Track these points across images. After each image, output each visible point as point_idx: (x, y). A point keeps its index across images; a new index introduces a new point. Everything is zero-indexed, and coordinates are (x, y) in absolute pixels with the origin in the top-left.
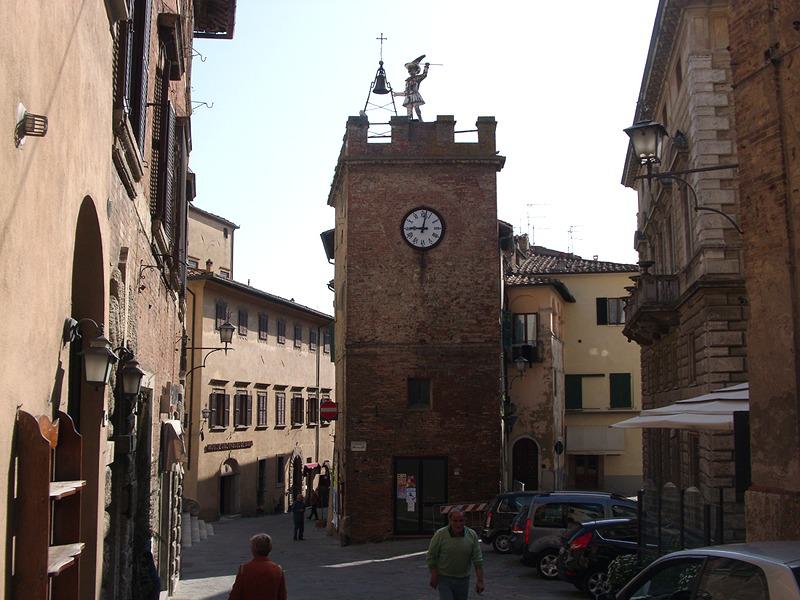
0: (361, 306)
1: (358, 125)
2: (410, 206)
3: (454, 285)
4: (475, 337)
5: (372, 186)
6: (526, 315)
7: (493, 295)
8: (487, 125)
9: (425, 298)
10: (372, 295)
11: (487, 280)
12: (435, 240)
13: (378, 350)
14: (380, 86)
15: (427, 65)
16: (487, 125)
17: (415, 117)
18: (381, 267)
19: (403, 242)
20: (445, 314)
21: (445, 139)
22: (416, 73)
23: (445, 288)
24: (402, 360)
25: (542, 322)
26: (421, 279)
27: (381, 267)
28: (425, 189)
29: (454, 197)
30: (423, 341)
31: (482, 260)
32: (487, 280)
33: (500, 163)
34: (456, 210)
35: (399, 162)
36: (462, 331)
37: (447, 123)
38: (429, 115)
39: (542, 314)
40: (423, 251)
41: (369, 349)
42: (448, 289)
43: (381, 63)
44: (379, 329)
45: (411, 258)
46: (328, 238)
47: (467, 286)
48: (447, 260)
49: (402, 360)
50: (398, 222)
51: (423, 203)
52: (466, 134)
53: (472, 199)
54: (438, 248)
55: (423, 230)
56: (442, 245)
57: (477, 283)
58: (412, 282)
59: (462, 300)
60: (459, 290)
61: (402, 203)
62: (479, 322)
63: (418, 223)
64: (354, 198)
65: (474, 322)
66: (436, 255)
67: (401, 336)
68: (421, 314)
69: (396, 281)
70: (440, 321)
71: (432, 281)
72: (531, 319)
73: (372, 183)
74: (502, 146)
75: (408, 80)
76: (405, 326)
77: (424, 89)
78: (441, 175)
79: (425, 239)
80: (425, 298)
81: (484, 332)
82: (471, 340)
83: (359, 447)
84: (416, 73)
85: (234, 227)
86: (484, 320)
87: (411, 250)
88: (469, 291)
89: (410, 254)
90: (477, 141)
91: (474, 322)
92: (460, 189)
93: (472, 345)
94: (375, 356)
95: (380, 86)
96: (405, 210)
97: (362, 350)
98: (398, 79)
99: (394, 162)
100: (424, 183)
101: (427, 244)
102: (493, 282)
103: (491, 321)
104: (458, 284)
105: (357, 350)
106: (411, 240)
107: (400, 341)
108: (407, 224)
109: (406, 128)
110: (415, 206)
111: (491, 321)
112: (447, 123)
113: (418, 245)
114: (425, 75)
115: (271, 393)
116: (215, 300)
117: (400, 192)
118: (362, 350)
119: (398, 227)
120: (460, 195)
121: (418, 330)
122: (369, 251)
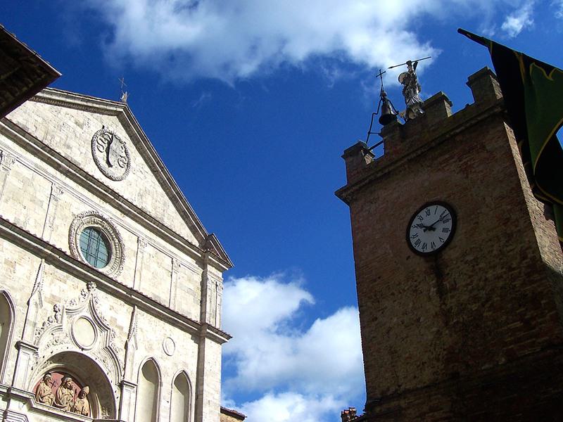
3: (482, 283)
7: (536, 277)
9: (446, 315)
10: (388, 332)
11: (524, 258)
12: (446, 236)
13: (403, 403)
18: (393, 294)
19: (412, 254)
21: (437, 120)
23: (473, 289)
24: (432, 410)
26: (441, 292)
27: (393, 294)
28: (427, 184)
37: (437, 102)
40: (437, 254)
42: (475, 292)
45: (424, 270)
47: (499, 278)
51: (427, 200)
54: (452, 244)
55: (432, 229)
57: (511, 269)
58: (430, 299)
59: (496, 299)
63: (428, 221)
65: (518, 324)
66: (451, 254)
67: (427, 376)
69: (411, 305)
71: (454, 288)
79: (434, 240)
87: (422, 260)
88: (501, 284)
89: (420, 265)
90: (471, 101)
91: (518, 324)
96: (409, 216)
99: (387, 171)
101: (439, 245)
102: (533, 259)
106: (419, 249)
110: (418, 207)
113: (429, 250)
119: (404, 240)
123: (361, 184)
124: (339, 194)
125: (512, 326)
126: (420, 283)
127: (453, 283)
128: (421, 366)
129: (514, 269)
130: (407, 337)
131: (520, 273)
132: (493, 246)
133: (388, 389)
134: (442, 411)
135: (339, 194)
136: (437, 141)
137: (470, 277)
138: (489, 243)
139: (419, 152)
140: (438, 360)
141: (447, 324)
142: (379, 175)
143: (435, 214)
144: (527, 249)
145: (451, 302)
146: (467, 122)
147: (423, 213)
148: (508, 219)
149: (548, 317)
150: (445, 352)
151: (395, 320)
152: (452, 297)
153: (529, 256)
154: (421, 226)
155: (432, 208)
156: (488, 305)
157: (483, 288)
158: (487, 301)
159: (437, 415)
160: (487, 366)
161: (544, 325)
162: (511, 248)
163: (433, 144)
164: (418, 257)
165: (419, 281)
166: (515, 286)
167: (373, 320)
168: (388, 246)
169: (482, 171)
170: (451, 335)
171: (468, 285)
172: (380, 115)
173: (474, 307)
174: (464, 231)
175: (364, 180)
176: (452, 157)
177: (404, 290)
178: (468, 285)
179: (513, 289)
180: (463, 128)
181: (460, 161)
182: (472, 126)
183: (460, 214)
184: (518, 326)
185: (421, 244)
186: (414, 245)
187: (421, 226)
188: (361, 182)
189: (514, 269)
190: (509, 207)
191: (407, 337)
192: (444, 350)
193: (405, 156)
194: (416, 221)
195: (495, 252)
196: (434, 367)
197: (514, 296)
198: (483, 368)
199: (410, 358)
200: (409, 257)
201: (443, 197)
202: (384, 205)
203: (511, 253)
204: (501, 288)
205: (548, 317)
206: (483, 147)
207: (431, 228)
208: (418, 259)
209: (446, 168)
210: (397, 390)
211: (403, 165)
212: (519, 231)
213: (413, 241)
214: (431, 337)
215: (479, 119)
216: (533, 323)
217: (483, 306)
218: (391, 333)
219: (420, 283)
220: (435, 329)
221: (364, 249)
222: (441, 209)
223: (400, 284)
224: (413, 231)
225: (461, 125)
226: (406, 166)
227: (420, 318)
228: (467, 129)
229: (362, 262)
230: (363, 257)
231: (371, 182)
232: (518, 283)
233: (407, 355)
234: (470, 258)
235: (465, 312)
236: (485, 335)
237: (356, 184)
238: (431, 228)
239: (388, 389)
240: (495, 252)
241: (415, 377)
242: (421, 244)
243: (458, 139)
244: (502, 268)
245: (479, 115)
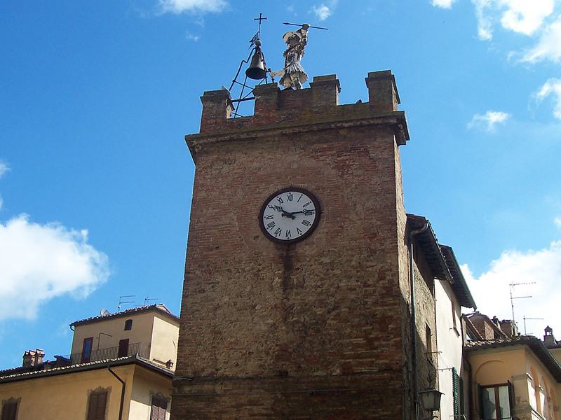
0: (199, 327)
1: (216, 99)
2: (272, 190)
3: (332, 289)
4: (361, 364)
5: (226, 168)
6: (496, 386)
7: (390, 300)
8: (381, 83)
9: (287, 311)
10: (216, 309)
11: (382, 278)
12: (305, 229)
13: (218, 389)
16: (381, 83)
18: (229, 271)
20: (318, 331)
21: (324, 103)
23: (321, 293)
24: (251, 403)
25: (517, 395)
26: (286, 285)
27: (229, 271)
28: (295, 166)
29: (334, 172)
30: (283, 374)
31: (373, 252)
32: (382, 278)
33: (398, 129)
34: (337, 187)
35: (260, 135)
36: (343, 357)
37: (328, 84)
39: (517, 383)
40: (290, 244)
41: (206, 387)
42: (324, 297)
43: (256, 41)
44: (221, 358)
47: (351, 289)
48: (321, 255)
49: (251, 403)
50: (256, 211)
51: (292, 183)
52: (352, 92)
53: (360, 172)
54: (310, 239)
55: (289, 217)
57: (366, 285)
58: (271, 288)
60: (338, 297)
61: (262, 186)
62: (370, 343)
63: (289, 207)
64: (203, 185)
66: (305, 250)
67: (252, 367)
68: (284, 335)
69: (249, 288)
70: (310, 342)
72: (504, 392)
73: (226, 166)
74: (408, 104)
75: (286, 53)
76: (259, 352)
78: (317, 146)
81: (378, 357)
82: (358, 369)
84: (296, 45)
86: (377, 339)
87: (272, 245)
88: (353, 296)
89: (269, 251)
90: (366, 99)
91: (361, 341)
92: (344, 161)
93: (357, 377)
94: (211, 398)
96: (267, 194)
97: (195, 389)
100: (293, 159)
101: (295, 235)
102: (391, 282)
103: (387, 339)
104: (338, 287)
105: (187, 389)
106: (272, 232)
107: (250, 375)
109: (274, 98)
110: (280, 187)
111: (387, 339)
112: (328, 84)
113: (282, 237)
114: (305, 43)
116: (151, 393)
117: (261, 173)
118: (195, 389)
119: (256, 217)
120: (342, 168)
121: (278, 358)
122: (214, 252)
123: (216, 138)
124: (189, 139)
125: (355, 341)
126: (264, 268)
127: (301, 279)
128: (247, 355)
129: (369, 286)
130: (237, 320)
131: (374, 292)
132: (353, 256)
133: (203, 370)
134: (262, 407)
135: (189, 139)
136: (321, 127)
137: (322, 279)
138: (350, 252)
139: (297, 130)
140: (268, 354)
141: (285, 319)
142: (242, 136)
143: (298, 202)
144: (387, 270)
145: (295, 299)
146: (358, 120)
147: (284, 196)
148: (375, 235)
149: (392, 342)
150: (278, 348)
151: (226, 299)
152: (297, 294)
153: (388, 278)
154: (279, 209)
155: (296, 195)
156: (334, 313)
157: (333, 295)
158: (334, 309)
159: (256, 409)
160: (319, 373)
161: (386, 348)
162: (369, 264)
163: (315, 128)
164: (268, 241)
165: (263, 265)
166: (367, 302)
167: (200, 292)
168: (235, 217)
169: (360, 176)
170: (288, 333)
171: (319, 287)
172: (247, 66)
173: (319, 311)
174: (325, 230)
175: (226, 135)
176: (330, 149)
177: (244, 270)
178: (319, 287)
179: (364, 305)
180: (352, 124)
181: (338, 157)
182: (361, 126)
183: (326, 211)
184: (360, 342)
185: (275, 229)
186: (266, 227)
187: (279, 209)
188: (221, 136)
189: (369, 286)
190: (379, 223)
191: (237, 320)
192: (277, 345)
193: (280, 129)
194: (274, 202)
195: (353, 263)
196: (261, 360)
197: (363, 312)
198: (315, 374)
199: (236, 343)
200: (258, 237)
201: (311, 187)
202: (241, 171)
203: (370, 269)
204: (352, 300)
205: (392, 342)
206: (367, 152)
207: (291, 216)
208: (267, 242)
209: (321, 158)
210: (212, 373)
211: (274, 136)
212: (383, 250)
213: (266, 222)
214: (264, 328)
215: (372, 122)
216: (376, 343)
217: (329, 312)
218: (219, 312)
219: (264, 268)
220: (271, 321)
221: (205, 211)
222: (306, 199)
223: (240, 262)
224: (268, 211)
225: (351, 121)
226: (276, 139)
227: (255, 306)
228: (355, 127)
229: (199, 224)
230: (201, 219)
231: (231, 140)
232: (370, 301)
233: (233, 340)
234: (326, 260)
235: (309, 313)
236: (324, 342)
237: (214, 136)
238: (291, 216)
239: (203, 370)
240: (353, 263)
241: (237, 365)
242: (275, 229)
243: (342, 132)
244: (357, 281)
245: (372, 119)
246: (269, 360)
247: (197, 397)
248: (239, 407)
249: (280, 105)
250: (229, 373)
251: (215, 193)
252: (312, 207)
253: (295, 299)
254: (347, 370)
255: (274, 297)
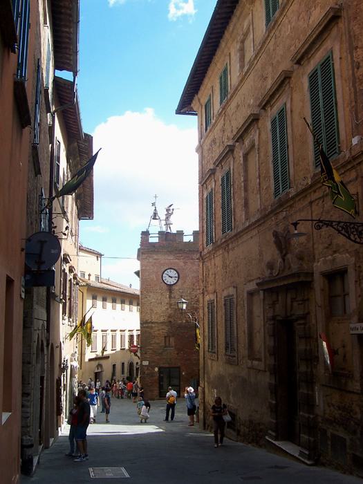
1: (145, 234)
9: (171, 305)
13: (153, 325)
14: (155, 216)
15: (173, 210)
17: (169, 231)
22: (169, 213)
24: (163, 329)
26: (170, 297)
37: (180, 234)
38: (174, 231)
46: (137, 273)
49: (163, 329)
56: (178, 284)
66: (174, 287)
67: (162, 319)
68: (169, 311)
71: (175, 298)
77: (172, 219)
79: (171, 281)
80: (171, 305)
83: (146, 363)
84: (169, 213)
85: (101, 255)
89: (165, 287)
94: (152, 328)
95: (155, 216)
96: (163, 270)
98: (162, 214)
101: (172, 283)
108: (166, 272)
112: (180, 234)
113: (169, 283)
115: (118, 334)
120: (185, 263)
121: (169, 317)
123: (147, 250)
159: (164, 331)
183: (181, 276)
201: (176, 268)
246: (166, 318)
247: (147, 327)
248: (159, 330)
249: (166, 240)
250: (156, 321)
251: (148, 268)
252: (177, 275)
253: (173, 302)
254: (187, 321)
255: (167, 300)
